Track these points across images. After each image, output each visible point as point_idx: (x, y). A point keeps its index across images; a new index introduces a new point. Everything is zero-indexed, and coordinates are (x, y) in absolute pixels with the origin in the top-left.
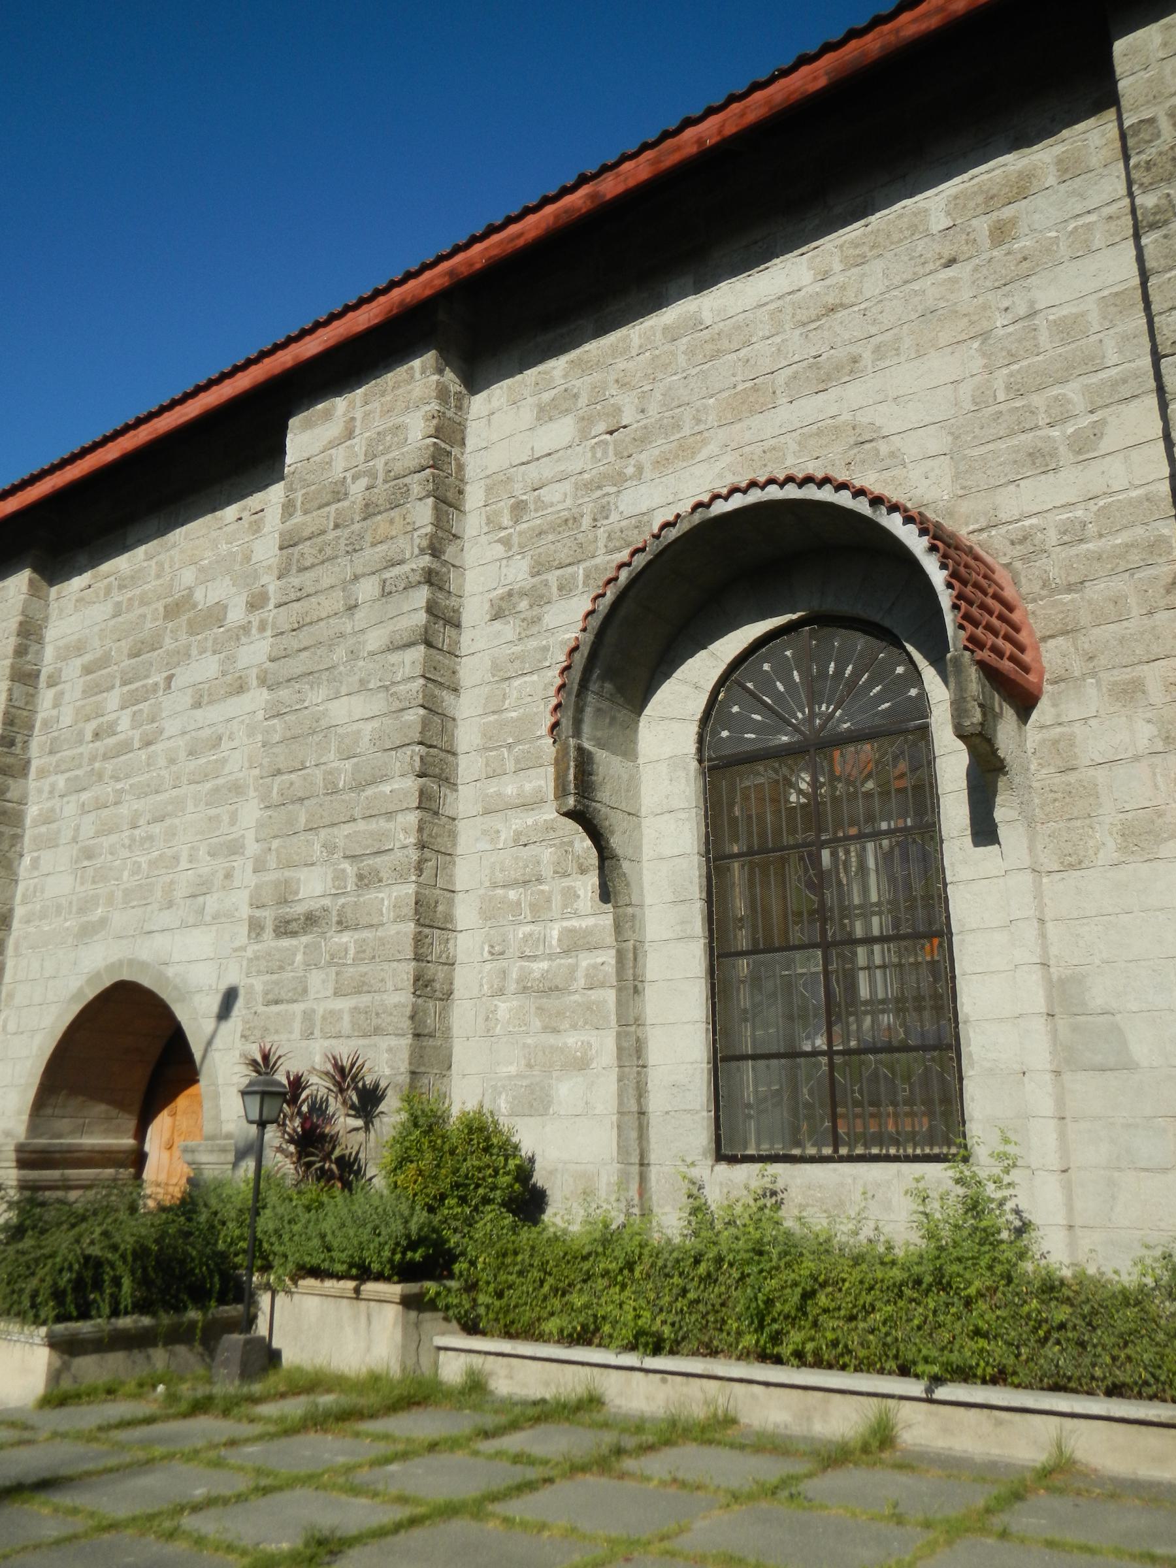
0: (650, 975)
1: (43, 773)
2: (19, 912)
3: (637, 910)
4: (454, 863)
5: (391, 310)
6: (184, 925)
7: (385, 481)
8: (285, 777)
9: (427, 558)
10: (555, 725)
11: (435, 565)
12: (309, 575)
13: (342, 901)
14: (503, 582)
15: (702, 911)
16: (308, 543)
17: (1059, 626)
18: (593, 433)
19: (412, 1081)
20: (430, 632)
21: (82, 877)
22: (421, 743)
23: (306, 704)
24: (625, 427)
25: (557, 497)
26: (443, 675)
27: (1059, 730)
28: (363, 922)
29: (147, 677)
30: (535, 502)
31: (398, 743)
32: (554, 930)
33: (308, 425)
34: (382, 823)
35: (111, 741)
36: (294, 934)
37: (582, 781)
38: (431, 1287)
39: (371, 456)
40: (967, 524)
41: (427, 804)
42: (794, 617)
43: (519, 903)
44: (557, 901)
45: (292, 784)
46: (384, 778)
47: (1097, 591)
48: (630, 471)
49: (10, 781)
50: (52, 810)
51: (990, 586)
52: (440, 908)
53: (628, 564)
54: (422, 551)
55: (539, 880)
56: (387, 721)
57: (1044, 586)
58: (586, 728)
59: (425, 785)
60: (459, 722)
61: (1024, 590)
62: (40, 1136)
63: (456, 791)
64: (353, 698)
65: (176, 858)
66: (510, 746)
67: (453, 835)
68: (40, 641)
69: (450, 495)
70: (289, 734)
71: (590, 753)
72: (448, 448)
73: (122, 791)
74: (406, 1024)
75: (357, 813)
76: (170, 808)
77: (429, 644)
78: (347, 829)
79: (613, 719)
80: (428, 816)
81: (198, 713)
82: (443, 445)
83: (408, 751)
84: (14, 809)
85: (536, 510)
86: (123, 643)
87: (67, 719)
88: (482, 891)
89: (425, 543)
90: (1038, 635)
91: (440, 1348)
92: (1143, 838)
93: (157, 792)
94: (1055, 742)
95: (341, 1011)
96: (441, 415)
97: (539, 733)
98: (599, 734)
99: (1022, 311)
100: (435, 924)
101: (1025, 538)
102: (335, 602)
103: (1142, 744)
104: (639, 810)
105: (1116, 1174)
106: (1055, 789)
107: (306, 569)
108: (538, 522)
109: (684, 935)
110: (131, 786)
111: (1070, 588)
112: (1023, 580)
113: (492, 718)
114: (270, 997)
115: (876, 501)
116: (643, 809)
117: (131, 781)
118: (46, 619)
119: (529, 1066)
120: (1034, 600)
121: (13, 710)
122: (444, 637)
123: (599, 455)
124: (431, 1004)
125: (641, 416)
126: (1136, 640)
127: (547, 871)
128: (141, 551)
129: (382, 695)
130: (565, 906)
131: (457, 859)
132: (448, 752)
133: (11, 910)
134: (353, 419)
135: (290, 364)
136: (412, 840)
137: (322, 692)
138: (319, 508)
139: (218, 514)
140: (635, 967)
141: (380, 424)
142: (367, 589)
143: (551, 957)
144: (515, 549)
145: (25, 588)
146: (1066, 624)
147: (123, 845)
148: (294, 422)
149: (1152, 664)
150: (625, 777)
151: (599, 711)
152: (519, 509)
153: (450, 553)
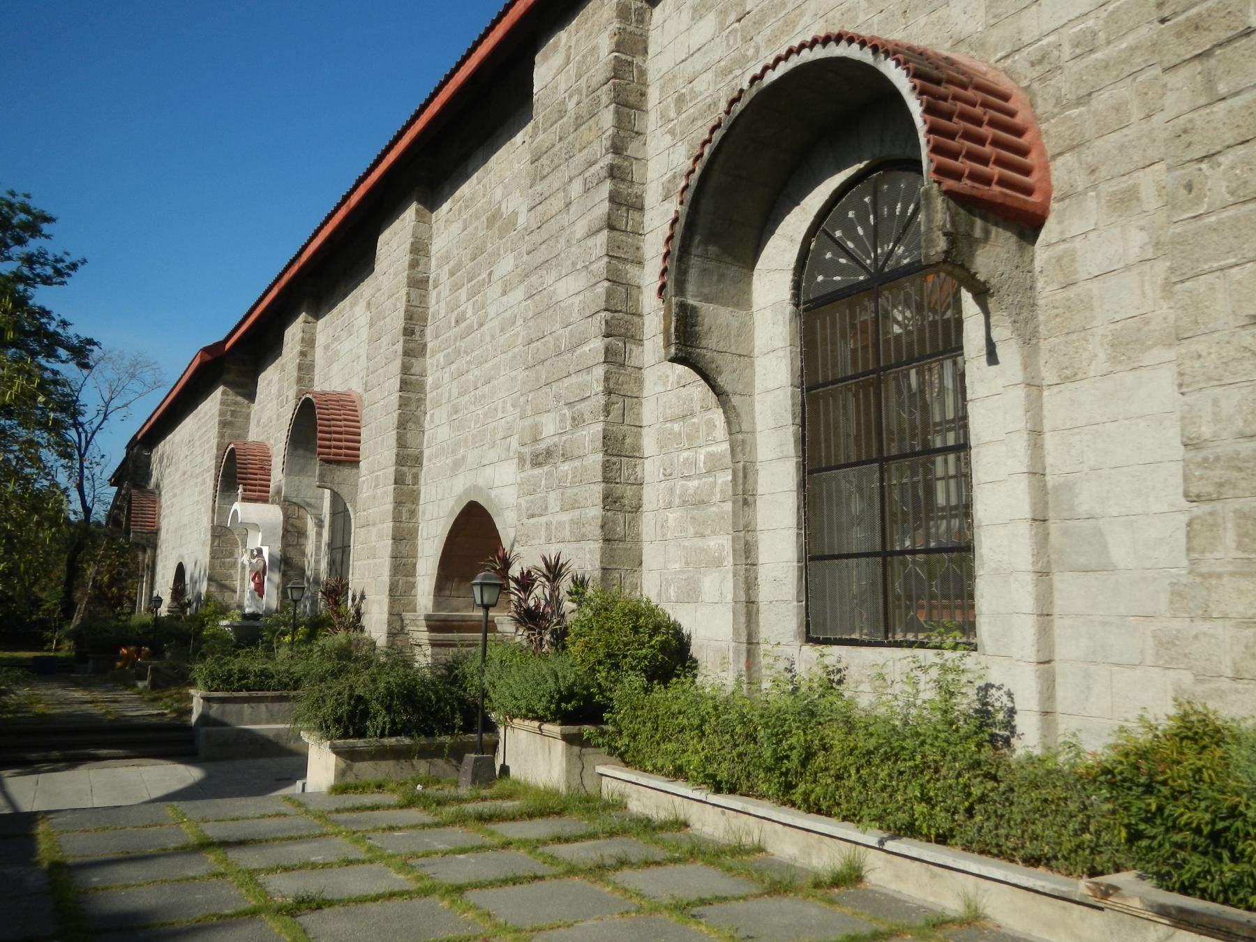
0: (761, 489)
1: (433, 353)
2: (426, 453)
3: (747, 437)
4: (641, 404)
6: (500, 460)
7: (587, 96)
8: (535, 344)
9: (610, 156)
10: (662, 288)
11: (618, 161)
12: (546, 182)
13: (564, 438)
14: (671, 167)
15: (794, 435)
16: (545, 156)
17: (1068, 142)
18: (728, 24)
19: (603, 574)
20: (613, 217)
22: (606, 310)
24: (748, 13)
25: (705, 85)
26: (626, 252)
27: (1063, 246)
28: (575, 454)
29: (479, 275)
30: (690, 94)
31: (593, 312)
32: (702, 456)
33: (545, 59)
35: (463, 325)
36: (540, 465)
37: (684, 333)
38: (588, 729)
39: (579, 77)
40: (996, 52)
41: (613, 358)
42: (861, 166)
43: (680, 434)
44: (703, 429)
47: (1101, 101)
48: (751, 52)
49: (413, 360)
51: (985, 114)
52: (628, 441)
53: (709, 141)
54: (607, 152)
55: (692, 415)
56: (588, 294)
57: (1057, 104)
58: (691, 287)
59: (610, 343)
60: (644, 289)
61: (1039, 111)
62: (443, 610)
63: (642, 345)
64: (571, 278)
65: (496, 410)
67: (639, 382)
68: (427, 255)
69: (631, 99)
70: (536, 311)
71: (694, 308)
72: (629, 59)
73: (469, 363)
74: (598, 532)
76: (493, 372)
77: (612, 227)
78: (567, 382)
79: (722, 277)
80: (613, 369)
81: (505, 298)
82: (624, 57)
83: (598, 316)
84: (417, 380)
85: (691, 101)
86: (467, 251)
87: (442, 313)
88: (658, 425)
89: (609, 143)
90: (1050, 153)
91: (602, 775)
92: (1130, 346)
94: (1059, 259)
95: (564, 522)
96: (620, 32)
98: (706, 290)
100: (623, 454)
101: (1043, 57)
102: (557, 203)
103: (1134, 253)
104: (752, 351)
105: (1093, 667)
106: (1056, 305)
107: (545, 177)
108: (692, 110)
109: (781, 455)
111: (1079, 102)
112: (1039, 100)
114: (530, 512)
116: (756, 350)
117: (474, 354)
118: (430, 237)
119: (687, 564)
120: (1047, 120)
121: (412, 308)
122: (626, 219)
123: (731, 43)
124: (620, 516)
126: (1135, 147)
127: (697, 408)
128: (474, 177)
129: (584, 273)
130: (708, 435)
131: (644, 401)
132: (634, 314)
133: (422, 452)
134: (570, 47)
136: (601, 388)
137: (554, 275)
138: (552, 125)
139: (513, 140)
140: (744, 483)
141: (584, 48)
142: (576, 188)
143: (700, 476)
144: (678, 137)
145: (413, 218)
146: (1073, 140)
148: (538, 58)
149: (1148, 169)
150: (736, 324)
151: (704, 272)
152: (681, 100)
153: (632, 149)
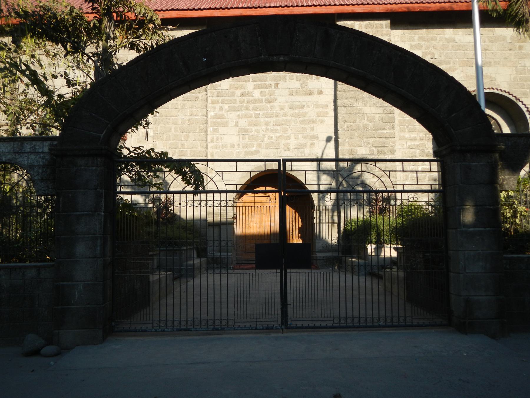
5: (388, 10)
21: (242, 137)
23: (354, 106)
29: (264, 81)
34: (384, 140)
45: (351, 125)
46: (384, 129)
50: (222, 115)
66: (407, 126)
75: (375, 136)
78: (373, 139)
81: (292, 97)
93: (276, 117)
97: (415, 124)
99: (523, 65)
110: (263, 113)
115: (516, 99)
125: (439, 57)
129: (381, 109)
135: (350, 11)
147: (263, 130)
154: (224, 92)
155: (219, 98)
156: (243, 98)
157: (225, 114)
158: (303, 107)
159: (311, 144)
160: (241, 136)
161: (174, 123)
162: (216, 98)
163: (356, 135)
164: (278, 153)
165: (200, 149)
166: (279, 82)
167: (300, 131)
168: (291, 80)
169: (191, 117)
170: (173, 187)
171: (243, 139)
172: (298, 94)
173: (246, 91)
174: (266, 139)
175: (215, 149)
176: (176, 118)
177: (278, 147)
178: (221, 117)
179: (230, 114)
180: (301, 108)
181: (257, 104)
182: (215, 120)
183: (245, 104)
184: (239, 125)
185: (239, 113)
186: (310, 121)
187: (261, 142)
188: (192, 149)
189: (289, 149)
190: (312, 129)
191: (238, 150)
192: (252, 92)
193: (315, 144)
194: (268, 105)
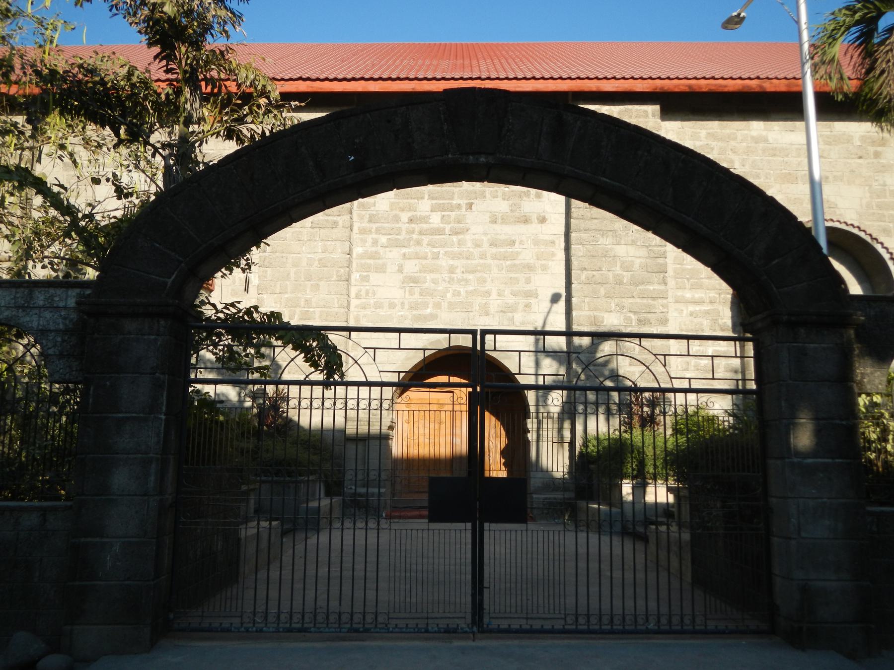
5: (656, 89)
21: (410, 291)
23: (599, 243)
34: (650, 301)
45: (594, 276)
46: (649, 283)
50: (376, 252)
66: (688, 279)
70: (589, 254)
75: (635, 294)
78: (630, 300)
81: (495, 226)
93: (467, 259)
97: (701, 277)
99: (881, 182)
110: (446, 252)
113: (678, 266)
115: (872, 239)
125: (742, 167)
129: (645, 249)
135: (594, 89)
147: (444, 280)
154: (380, 216)
155: (371, 225)
156: (413, 225)
157: (381, 251)
158: (513, 243)
159: (526, 306)
160: (407, 289)
161: (295, 265)
162: (368, 225)
163: (602, 291)
164: (469, 319)
165: (336, 310)
166: (473, 201)
167: (506, 283)
168: (494, 197)
169: (323, 256)
170: (289, 373)
171: (411, 294)
172: (504, 221)
173: (418, 214)
174: (449, 295)
175: (362, 310)
176: (299, 255)
177: (470, 310)
178: (374, 256)
179: (390, 251)
180: (510, 245)
181: (436, 237)
182: (363, 261)
183: (415, 236)
184: (405, 271)
185: (404, 250)
186: (524, 267)
187: (440, 301)
188: (324, 309)
189: (487, 314)
190: (528, 281)
191: (400, 311)
192: (428, 217)
193: (532, 306)
194: (455, 239)
